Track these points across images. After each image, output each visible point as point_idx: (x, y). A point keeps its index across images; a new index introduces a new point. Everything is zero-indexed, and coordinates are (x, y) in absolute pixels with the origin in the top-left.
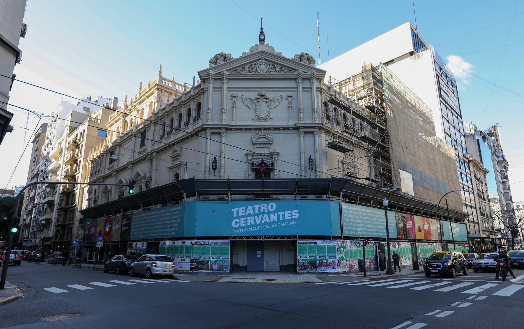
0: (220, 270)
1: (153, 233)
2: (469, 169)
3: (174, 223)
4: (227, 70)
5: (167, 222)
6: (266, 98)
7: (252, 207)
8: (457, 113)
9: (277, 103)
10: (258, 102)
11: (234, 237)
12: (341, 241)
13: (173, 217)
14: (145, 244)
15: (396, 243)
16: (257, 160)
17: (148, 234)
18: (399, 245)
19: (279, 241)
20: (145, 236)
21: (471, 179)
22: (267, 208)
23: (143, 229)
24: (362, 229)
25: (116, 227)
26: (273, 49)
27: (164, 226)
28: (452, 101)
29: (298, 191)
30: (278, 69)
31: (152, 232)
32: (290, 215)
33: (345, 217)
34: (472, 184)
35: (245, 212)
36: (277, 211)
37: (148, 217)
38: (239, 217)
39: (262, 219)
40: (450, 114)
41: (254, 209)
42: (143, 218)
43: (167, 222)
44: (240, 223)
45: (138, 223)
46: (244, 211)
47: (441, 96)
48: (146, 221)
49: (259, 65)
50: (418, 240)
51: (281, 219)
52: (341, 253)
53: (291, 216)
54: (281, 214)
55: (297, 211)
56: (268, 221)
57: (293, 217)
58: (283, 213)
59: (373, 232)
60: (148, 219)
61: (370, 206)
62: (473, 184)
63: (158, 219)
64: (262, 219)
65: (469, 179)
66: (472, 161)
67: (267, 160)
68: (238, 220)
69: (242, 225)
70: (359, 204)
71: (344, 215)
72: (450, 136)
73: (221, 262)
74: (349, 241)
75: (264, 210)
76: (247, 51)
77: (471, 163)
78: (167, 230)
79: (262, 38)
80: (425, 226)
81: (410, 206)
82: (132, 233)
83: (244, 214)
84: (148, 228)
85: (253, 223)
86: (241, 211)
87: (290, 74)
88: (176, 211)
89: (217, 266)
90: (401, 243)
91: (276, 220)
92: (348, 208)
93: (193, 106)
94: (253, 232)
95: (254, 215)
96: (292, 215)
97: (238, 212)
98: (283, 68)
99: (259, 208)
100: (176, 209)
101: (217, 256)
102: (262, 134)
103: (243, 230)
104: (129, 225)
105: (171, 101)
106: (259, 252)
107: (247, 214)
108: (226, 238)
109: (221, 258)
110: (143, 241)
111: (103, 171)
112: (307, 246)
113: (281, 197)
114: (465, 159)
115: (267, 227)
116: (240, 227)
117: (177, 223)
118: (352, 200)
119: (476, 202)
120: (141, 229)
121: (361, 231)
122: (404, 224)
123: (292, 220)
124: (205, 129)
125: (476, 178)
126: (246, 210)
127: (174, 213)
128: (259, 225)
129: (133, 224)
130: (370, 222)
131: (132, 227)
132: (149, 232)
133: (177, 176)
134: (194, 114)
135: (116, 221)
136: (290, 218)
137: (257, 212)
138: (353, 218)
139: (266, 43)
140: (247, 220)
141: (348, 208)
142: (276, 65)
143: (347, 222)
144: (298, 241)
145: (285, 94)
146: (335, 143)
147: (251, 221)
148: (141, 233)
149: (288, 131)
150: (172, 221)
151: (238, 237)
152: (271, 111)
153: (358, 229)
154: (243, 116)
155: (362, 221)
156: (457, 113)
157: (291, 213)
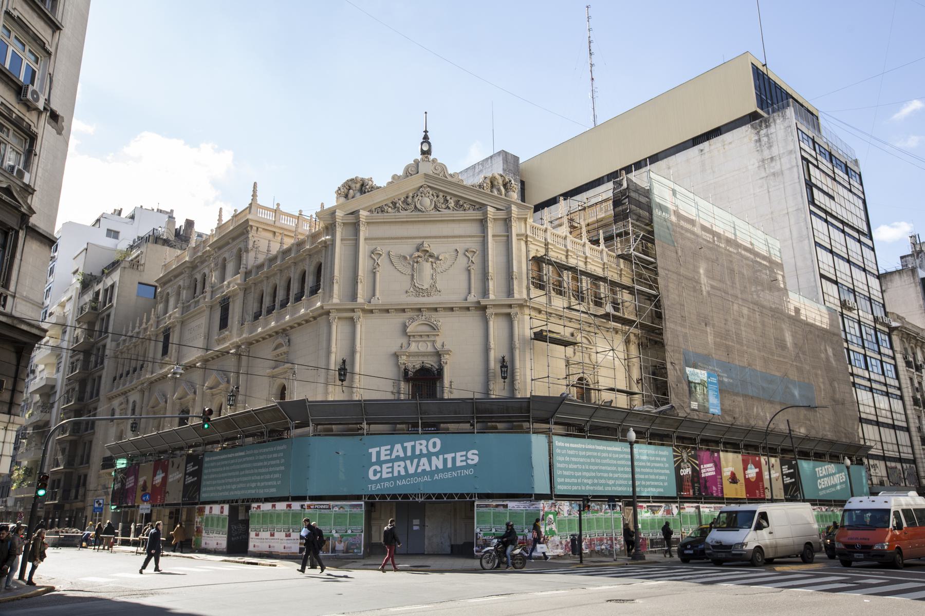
0: (347, 552)
1: (241, 489)
2: (892, 348)
3: (275, 472)
4: (364, 209)
5: (263, 470)
7: (402, 446)
8: (858, 231)
9: (449, 263)
10: (417, 262)
11: (371, 497)
12: (550, 502)
13: (273, 462)
14: (226, 507)
15: (674, 506)
16: (414, 364)
17: (231, 490)
18: (680, 509)
19: (434, 503)
20: (227, 493)
21: (896, 367)
22: (427, 446)
23: (223, 481)
24: (596, 481)
25: (175, 476)
26: (443, 168)
27: (258, 478)
28: (846, 207)
29: (477, 418)
30: (453, 205)
31: (239, 486)
32: (464, 458)
33: (560, 462)
34: (898, 378)
35: (391, 454)
36: (443, 451)
37: (232, 461)
38: (380, 463)
39: (418, 465)
40: (837, 236)
41: (405, 449)
42: (223, 463)
43: (263, 470)
44: (381, 472)
45: (214, 470)
46: (388, 452)
47: (812, 201)
48: (228, 468)
50: (727, 499)
51: (450, 465)
52: (550, 523)
53: (466, 461)
54: (449, 456)
55: (476, 452)
56: (428, 469)
57: (470, 462)
58: (453, 455)
59: (621, 485)
60: (233, 464)
61: (616, 440)
62: (902, 377)
63: (249, 465)
64: (418, 465)
65: (887, 367)
66: (896, 328)
67: (430, 362)
68: (378, 468)
69: (385, 476)
70: (589, 437)
71: (557, 458)
72: (836, 283)
73: (350, 538)
74: (567, 503)
75: (421, 450)
76: (400, 172)
77: (895, 333)
78: (263, 484)
79: (425, 148)
80: (748, 471)
81: (707, 434)
82: (203, 489)
83: (388, 457)
84: (231, 480)
85: (403, 473)
86: (383, 453)
88: (277, 452)
89: (342, 544)
90: (686, 505)
91: (441, 467)
92: (567, 445)
93: (310, 269)
94: (402, 486)
95: (404, 459)
96: (467, 458)
97: (378, 453)
98: (461, 203)
99: (413, 448)
100: (279, 448)
101: (343, 528)
103: (387, 484)
104: (198, 474)
105: (274, 251)
106: (416, 522)
107: (393, 457)
108: (358, 498)
109: (349, 532)
110: (224, 502)
111: (149, 369)
112: (492, 510)
113: (452, 427)
114: (878, 326)
115: (426, 478)
116: (381, 480)
117: (280, 472)
118: (577, 430)
119: (910, 416)
120: (219, 482)
121: (593, 485)
122: (694, 469)
123: (468, 466)
124: (328, 313)
125: (908, 364)
126: (392, 450)
127: (275, 455)
128: (412, 475)
129: (205, 471)
130: (614, 468)
131: (204, 477)
132: (234, 487)
133: (283, 391)
134: (310, 281)
135: (176, 466)
136: (464, 464)
137: (409, 454)
138: (576, 463)
139: (431, 157)
140: (392, 467)
141: (567, 445)
142: (448, 198)
143: (561, 469)
144: (476, 504)
146: (545, 334)
147: (399, 469)
148: (219, 488)
150: (271, 469)
151: (377, 495)
153: (585, 481)
154: (392, 286)
155: (596, 467)
156: (858, 231)
157: (466, 456)
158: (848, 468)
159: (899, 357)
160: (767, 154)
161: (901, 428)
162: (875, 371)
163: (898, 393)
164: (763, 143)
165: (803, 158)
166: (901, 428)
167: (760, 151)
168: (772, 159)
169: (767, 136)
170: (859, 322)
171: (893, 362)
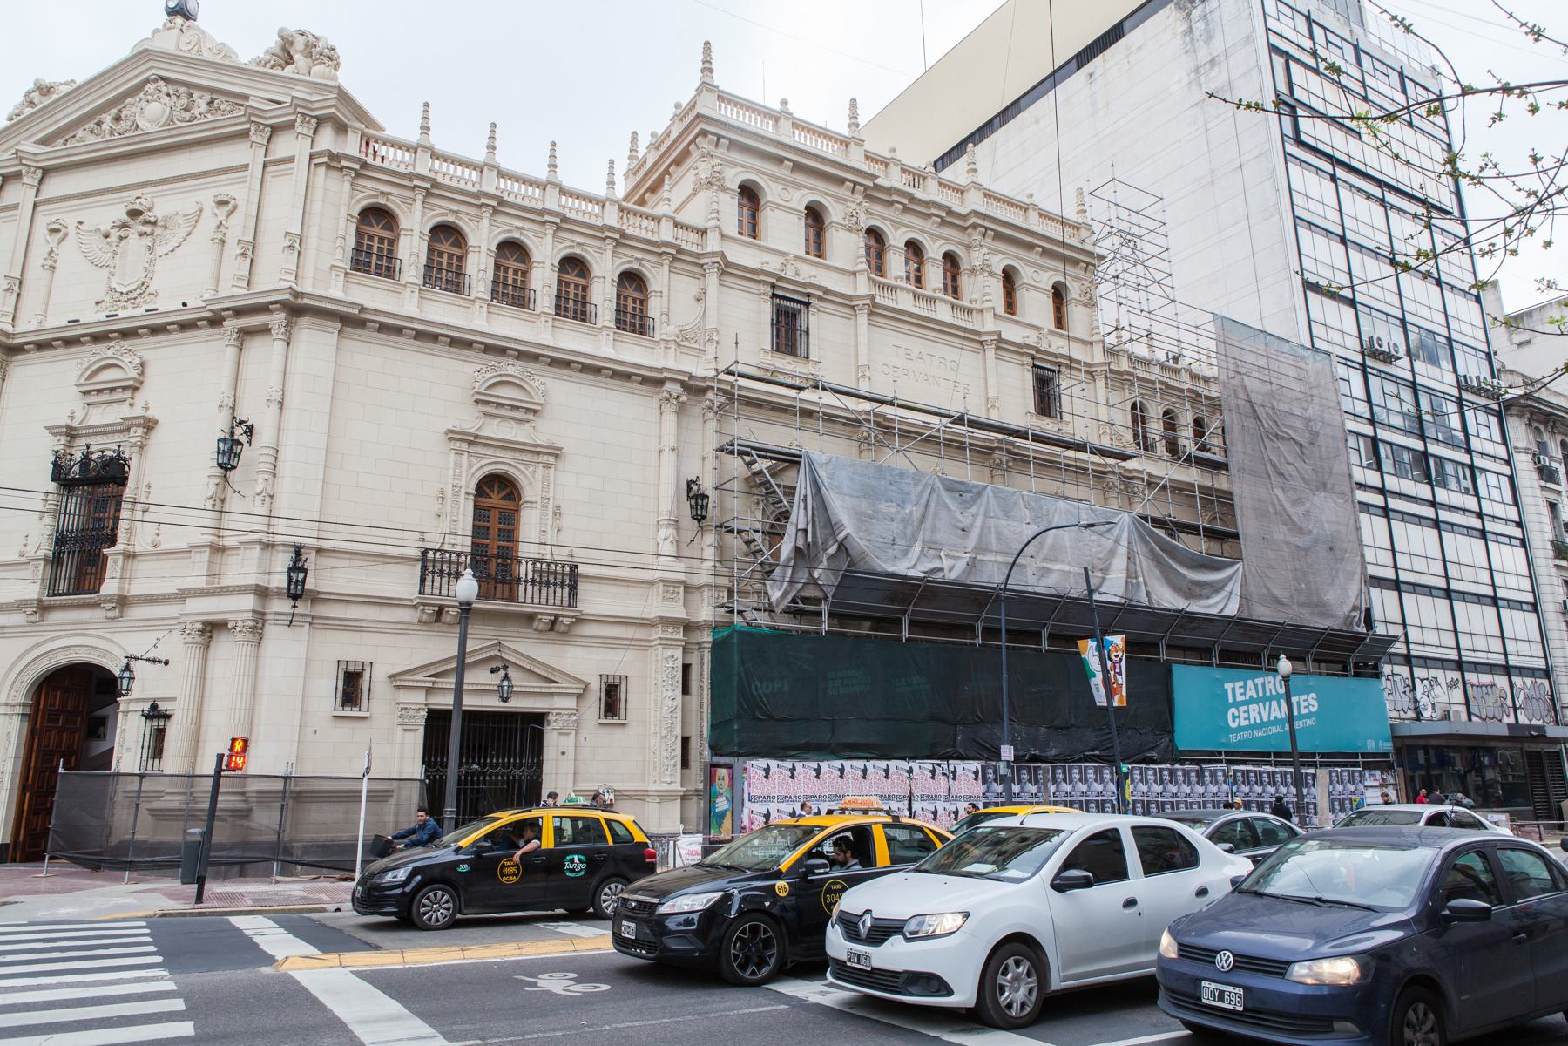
6: (146, 222)
9: (182, 233)
30: (204, 108)
49: (143, 104)
72: (1352, 303)
77: (1514, 411)
87: (234, 119)
102: (110, 353)
119: (1542, 580)
145: (205, 196)
149: (196, 333)
152: (159, 265)
158: (1286, 679)
159: (1524, 463)
160: (1203, 54)
161: (1514, 604)
162: (1495, 494)
163: (1517, 533)
164: (1196, 34)
165: (1273, 49)
166: (1514, 604)
167: (1191, 50)
168: (1213, 62)
169: (1204, 17)
170: (1414, 386)
171: (1506, 470)
